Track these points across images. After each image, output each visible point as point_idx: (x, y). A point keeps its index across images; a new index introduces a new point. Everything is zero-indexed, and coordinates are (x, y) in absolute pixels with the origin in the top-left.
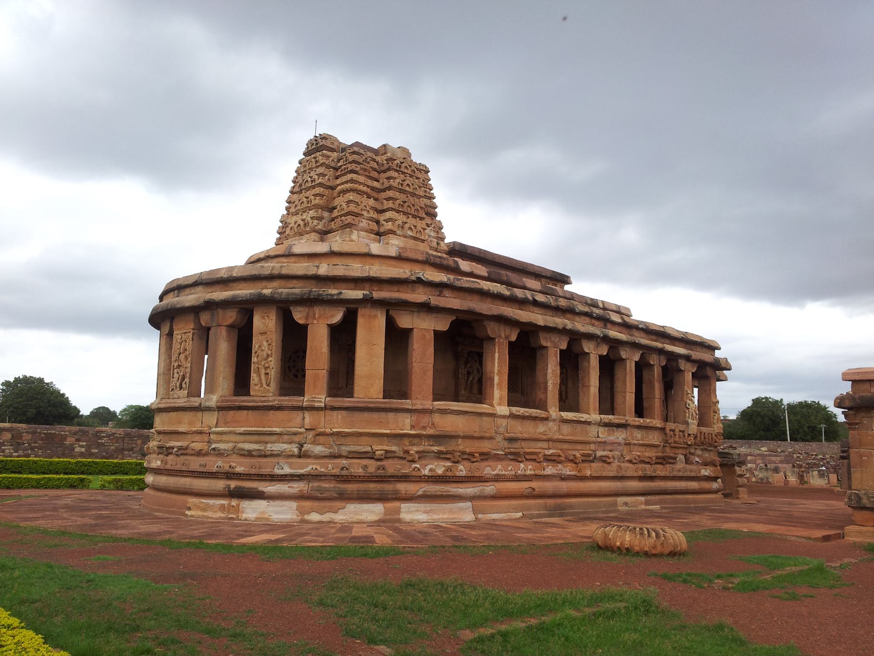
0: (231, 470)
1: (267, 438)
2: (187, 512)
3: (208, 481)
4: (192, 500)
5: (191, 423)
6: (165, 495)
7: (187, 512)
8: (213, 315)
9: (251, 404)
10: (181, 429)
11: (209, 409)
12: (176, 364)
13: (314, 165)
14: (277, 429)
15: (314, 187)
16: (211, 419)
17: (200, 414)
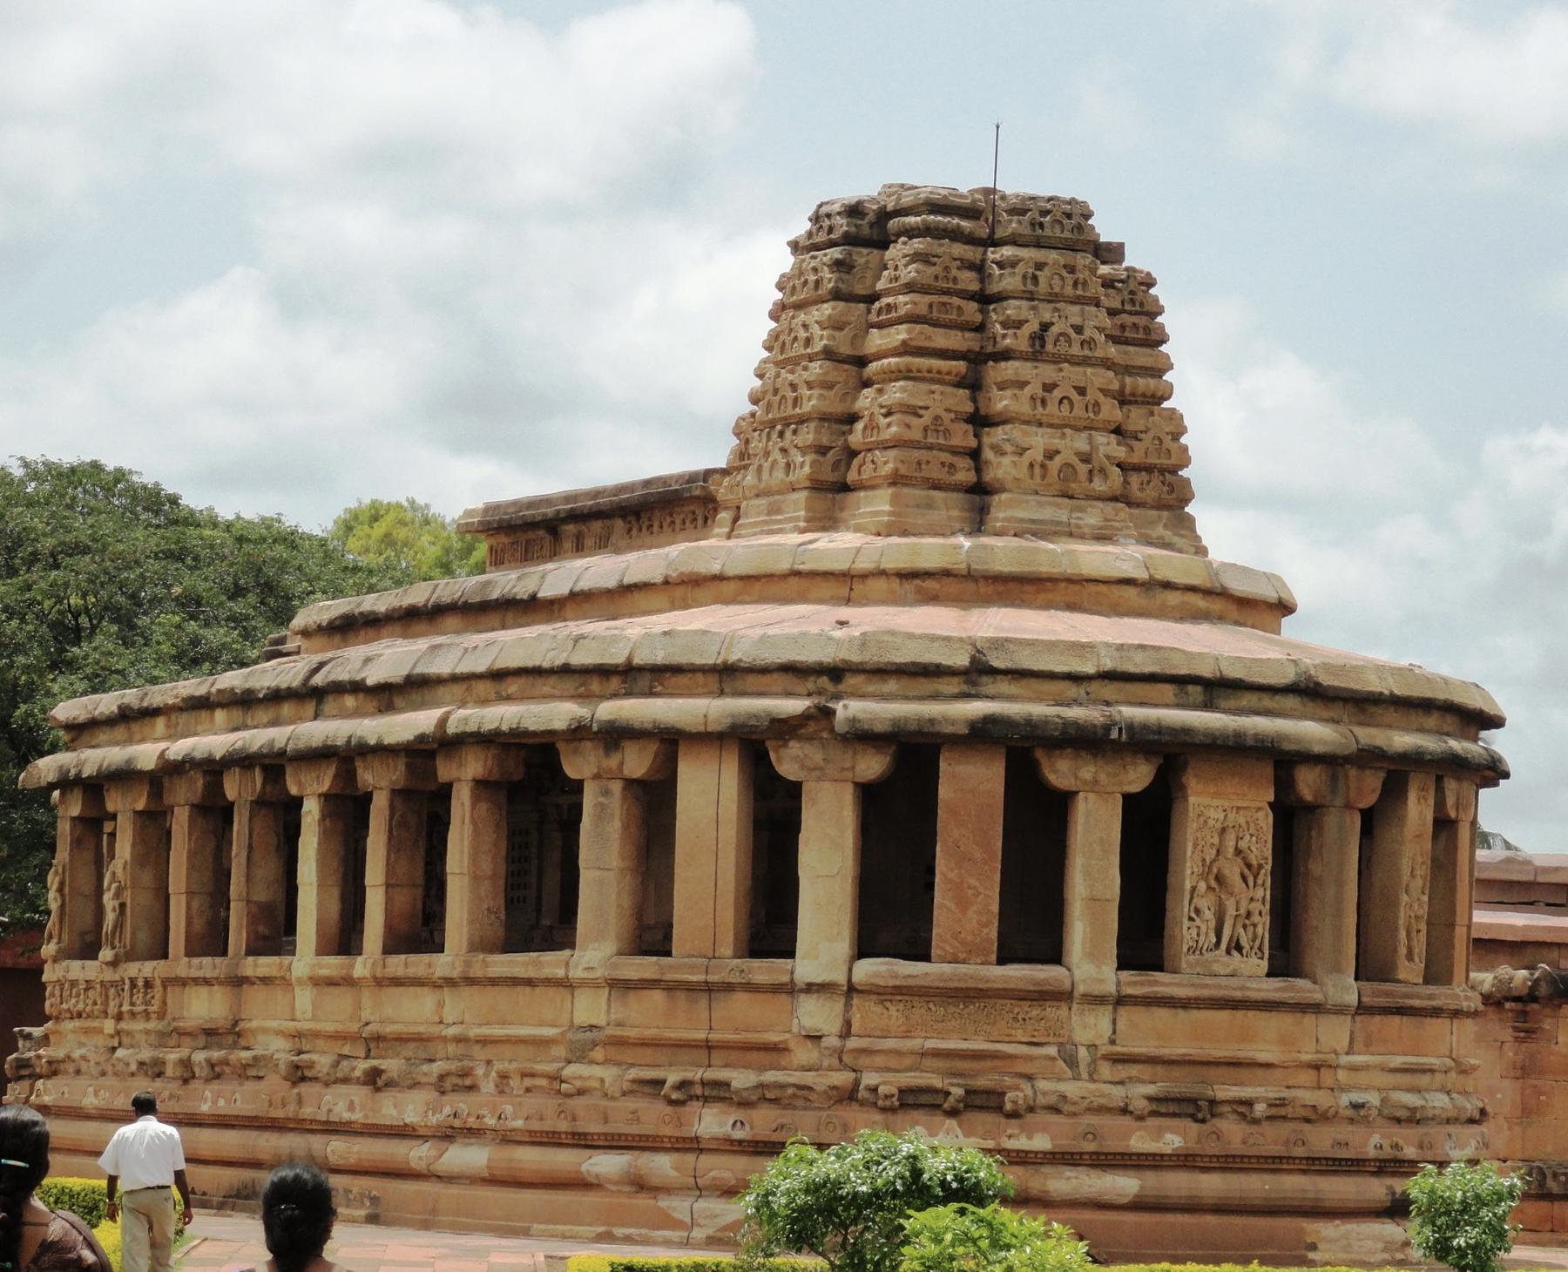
0: (1400, 1155)
1: (1424, 1080)
2: (1311, 1255)
3: (1267, 1177)
4: (1327, 1230)
5: (1285, 1041)
6: (1210, 1219)
7: (1311, 1255)
8: (1334, 779)
9: (1416, 1003)
10: (1263, 1057)
11: (1340, 1010)
12: (1202, 886)
13: (1069, 290)
14: (1433, 1060)
15: (1084, 362)
16: (1334, 1033)
17: (1309, 1020)
